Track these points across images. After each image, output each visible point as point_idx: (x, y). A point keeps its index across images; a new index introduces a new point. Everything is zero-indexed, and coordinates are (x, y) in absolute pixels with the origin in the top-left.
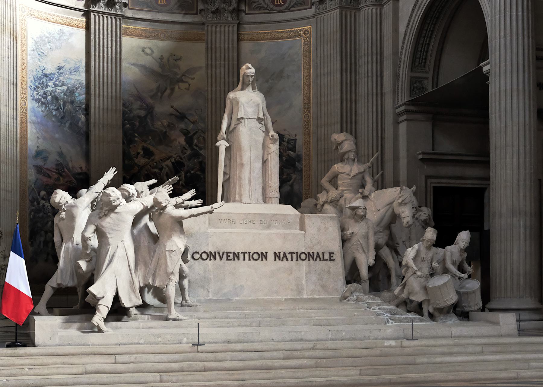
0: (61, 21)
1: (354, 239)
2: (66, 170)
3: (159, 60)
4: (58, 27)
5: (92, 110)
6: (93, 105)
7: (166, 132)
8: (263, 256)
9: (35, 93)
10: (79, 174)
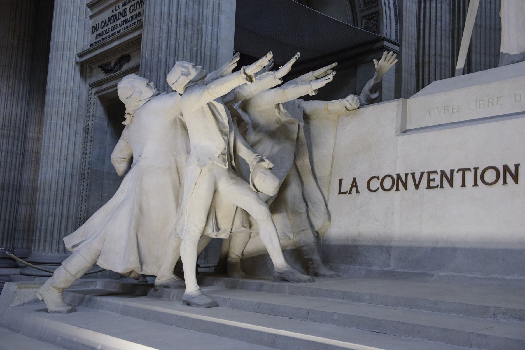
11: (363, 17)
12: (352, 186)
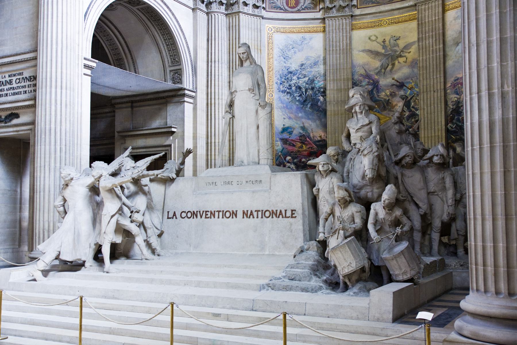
0: (303, 31)
1: (321, 195)
2: (308, 139)
3: (382, 43)
4: (301, 35)
5: (328, 92)
6: (328, 88)
7: (389, 100)
8: (234, 214)
9: (281, 86)
10: (319, 141)
11: (171, 71)
12: (174, 215)
